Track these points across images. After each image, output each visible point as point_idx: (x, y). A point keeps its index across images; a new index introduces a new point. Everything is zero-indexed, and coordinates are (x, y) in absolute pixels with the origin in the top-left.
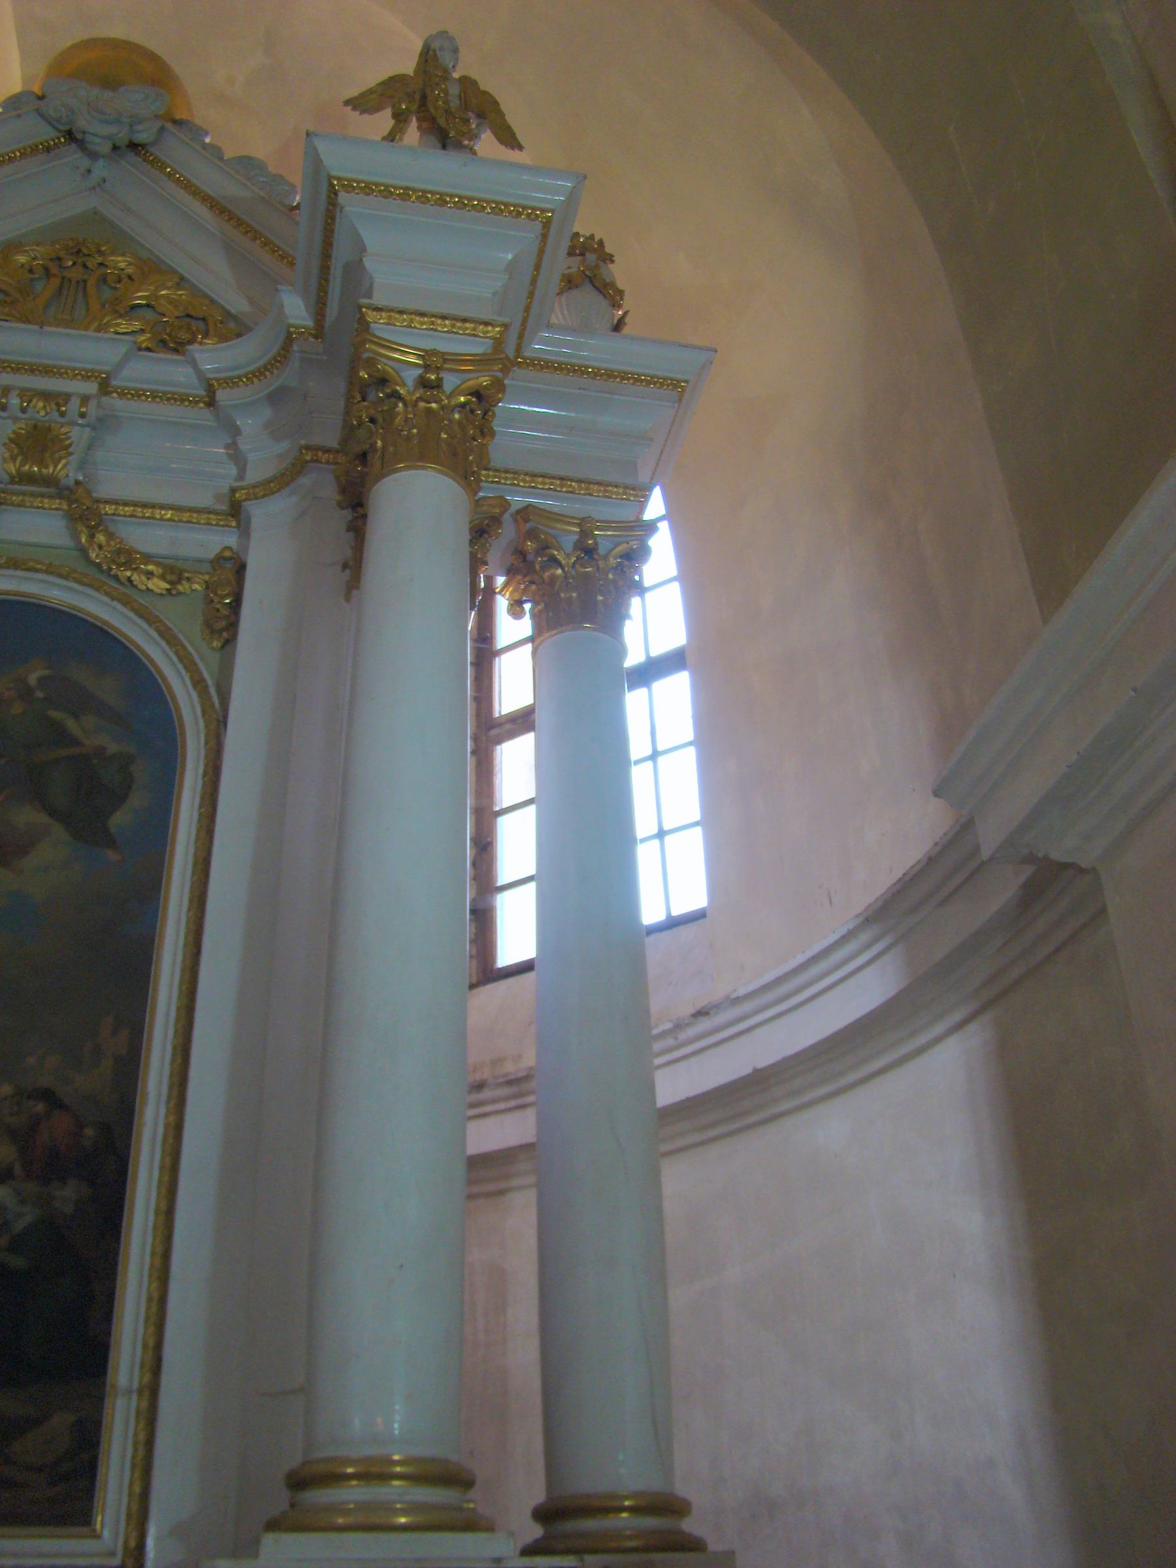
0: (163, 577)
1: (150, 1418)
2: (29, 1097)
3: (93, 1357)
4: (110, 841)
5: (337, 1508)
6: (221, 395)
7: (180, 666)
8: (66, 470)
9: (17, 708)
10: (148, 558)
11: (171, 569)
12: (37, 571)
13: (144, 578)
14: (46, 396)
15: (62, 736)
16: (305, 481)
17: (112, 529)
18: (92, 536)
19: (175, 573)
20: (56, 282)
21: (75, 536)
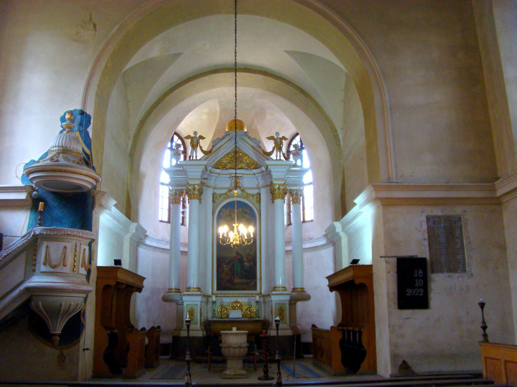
1: (261, 282)
19: (253, 196)
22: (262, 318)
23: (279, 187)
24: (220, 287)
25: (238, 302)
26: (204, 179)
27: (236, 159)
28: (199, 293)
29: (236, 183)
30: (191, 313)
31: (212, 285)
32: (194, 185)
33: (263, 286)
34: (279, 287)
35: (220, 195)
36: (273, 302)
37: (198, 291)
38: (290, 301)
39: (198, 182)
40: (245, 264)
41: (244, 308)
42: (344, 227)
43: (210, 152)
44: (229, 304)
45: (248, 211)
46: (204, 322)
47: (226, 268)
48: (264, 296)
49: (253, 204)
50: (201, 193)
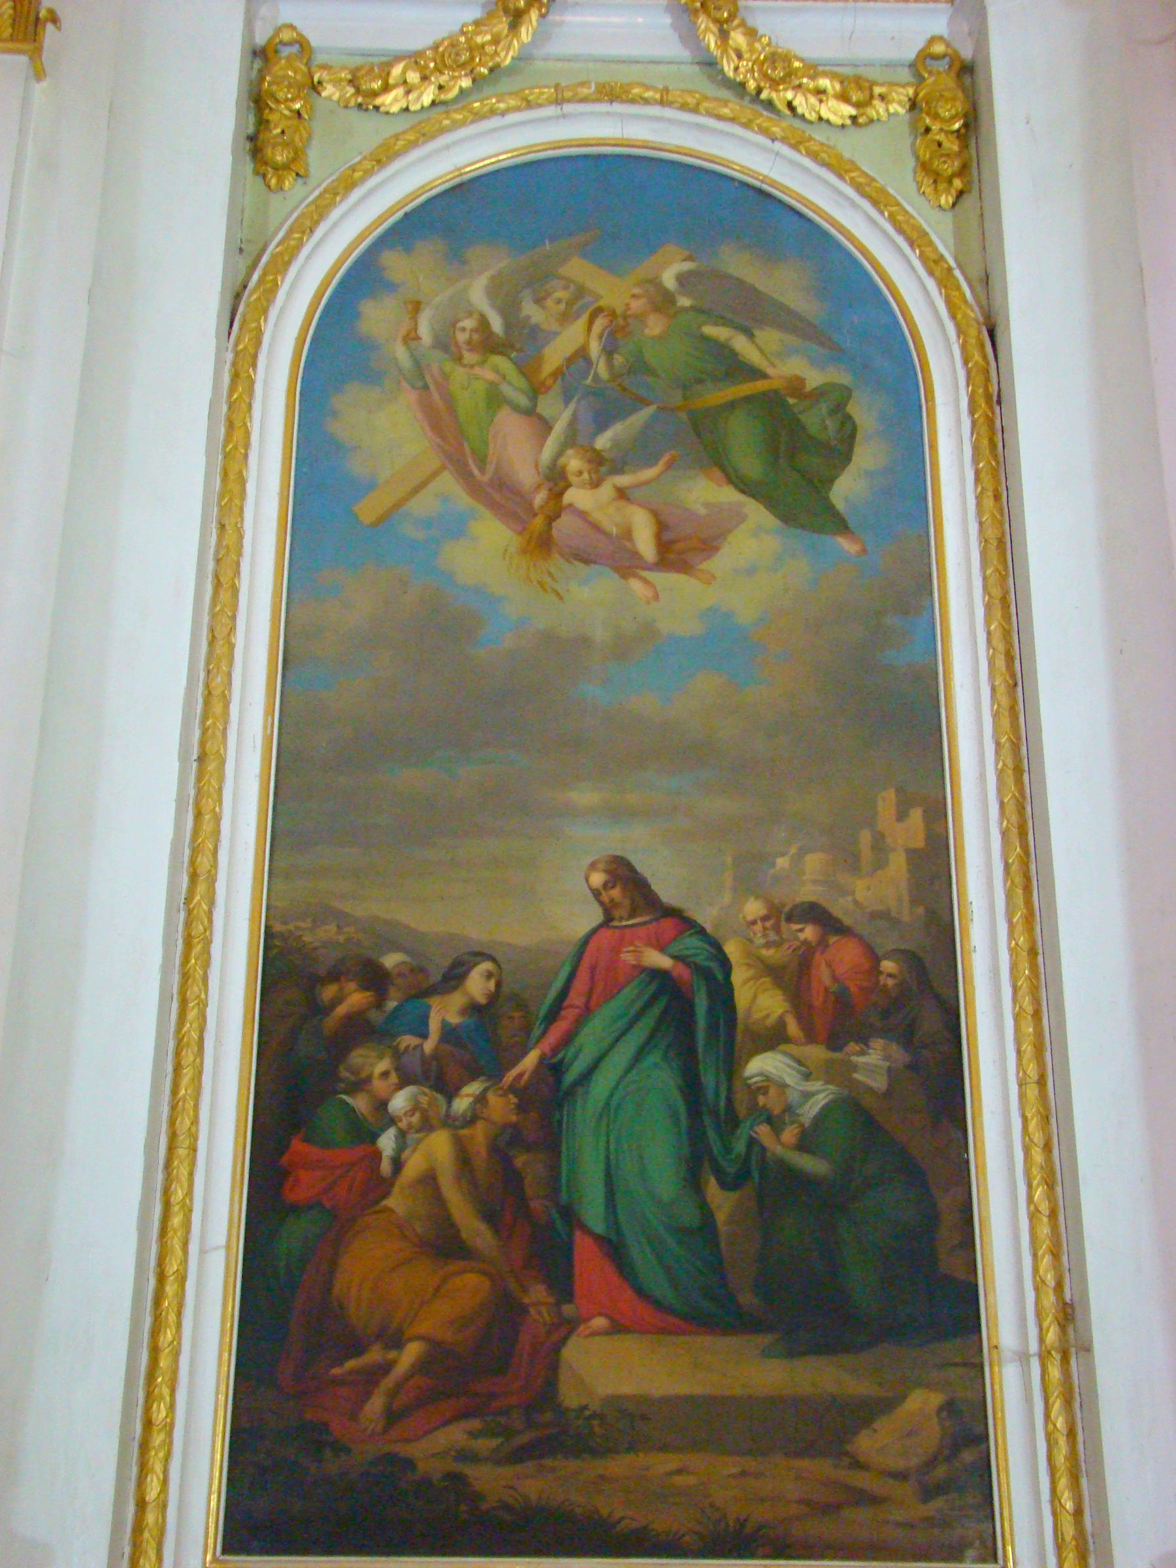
0: (844, 97)
2: (790, 919)
3: (950, 1308)
4: (841, 525)
7: (900, 240)
9: (655, 326)
10: (813, 69)
11: (858, 81)
12: (646, 102)
13: (813, 100)
15: (736, 369)
17: (751, 22)
18: (724, 35)
19: (858, 88)
21: (691, 38)
35: (367, 80)
40: (763, 1065)
45: (785, 285)
47: (422, 1141)
49: (879, 199)
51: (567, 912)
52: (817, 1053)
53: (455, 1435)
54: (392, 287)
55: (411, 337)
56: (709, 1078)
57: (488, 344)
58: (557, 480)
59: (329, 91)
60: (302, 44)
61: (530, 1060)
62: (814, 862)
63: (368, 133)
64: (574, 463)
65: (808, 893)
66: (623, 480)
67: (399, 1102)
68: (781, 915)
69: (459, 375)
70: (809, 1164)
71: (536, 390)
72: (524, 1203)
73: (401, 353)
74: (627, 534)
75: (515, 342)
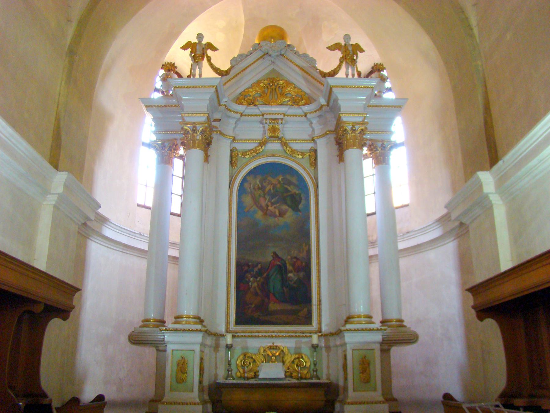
1: (320, 309)
4: (300, 211)
5: (353, 321)
6: (308, 115)
8: (280, 135)
9: (278, 186)
14: (274, 119)
15: (287, 190)
16: (328, 136)
19: (303, 154)
20: (270, 90)
21: (283, 147)
22: (324, 380)
23: (353, 126)
24: (243, 318)
25: (277, 348)
26: (215, 120)
27: (273, 88)
28: (199, 327)
29: (274, 130)
30: (182, 366)
31: (228, 315)
32: (194, 124)
33: (324, 315)
34: (359, 316)
35: (244, 153)
36: (349, 347)
37: (195, 323)
38: (382, 343)
39: (203, 119)
40: (290, 275)
41: (289, 359)
42: (500, 182)
43: (227, 73)
44: (259, 350)
45: (294, 180)
46: (210, 386)
47: (254, 283)
48: (325, 336)
49: (304, 168)
50: (207, 144)
51: (270, 258)
52: (296, 274)
53: (258, 313)
54: (247, 181)
55: (250, 188)
56: (284, 276)
57: (259, 188)
58: (267, 206)
59: (240, 155)
60: (236, 149)
61: (265, 275)
62: (296, 252)
63: (244, 161)
64: (269, 204)
65: (295, 255)
66: (275, 206)
67: (251, 279)
68: (292, 258)
69: (256, 193)
70: (295, 285)
71: (265, 195)
72: (264, 287)
73: (249, 190)
74: (275, 212)
75: (262, 188)
